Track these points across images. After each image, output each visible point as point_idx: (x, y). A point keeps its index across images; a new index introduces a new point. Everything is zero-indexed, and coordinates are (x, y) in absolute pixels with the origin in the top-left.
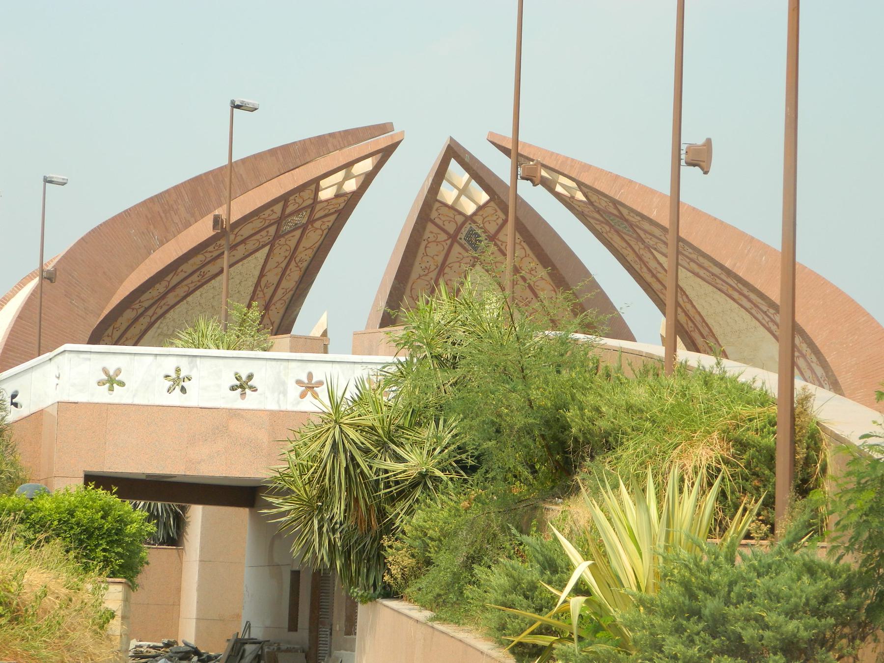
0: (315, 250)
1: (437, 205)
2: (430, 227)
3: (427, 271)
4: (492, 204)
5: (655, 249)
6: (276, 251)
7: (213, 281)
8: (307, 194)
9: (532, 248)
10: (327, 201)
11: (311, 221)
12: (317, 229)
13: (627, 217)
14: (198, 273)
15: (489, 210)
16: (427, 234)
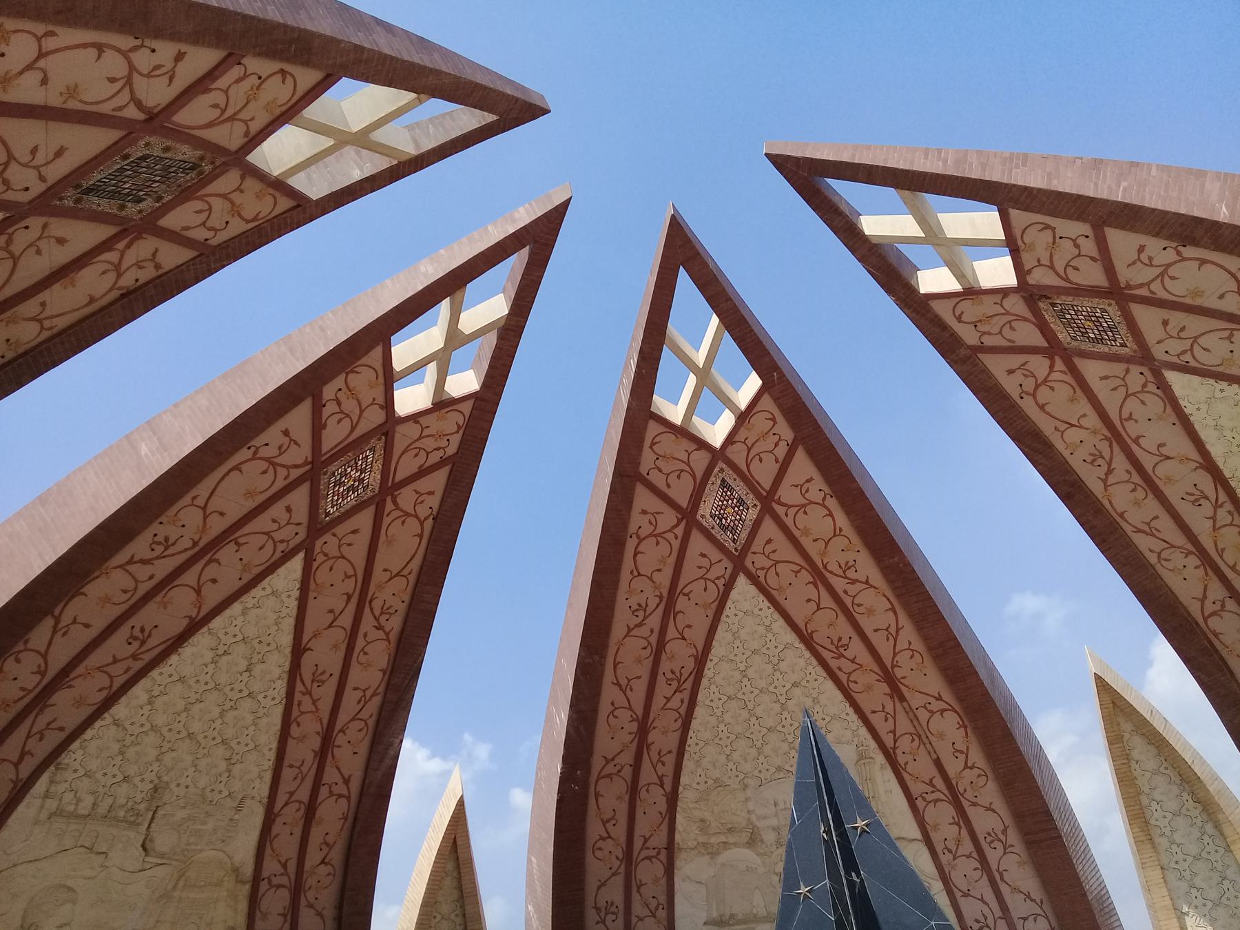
0: (412, 578)
1: (653, 429)
2: (643, 499)
3: (641, 614)
4: (767, 402)
5: (1185, 369)
6: (322, 575)
7: (174, 659)
8: (364, 379)
9: (848, 512)
10: (415, 417)
11: (389, 488)
12: (407, 514)
13: (1125, 275)
14: (123, 632)
15: (760, 422)
16: (637, 521)
